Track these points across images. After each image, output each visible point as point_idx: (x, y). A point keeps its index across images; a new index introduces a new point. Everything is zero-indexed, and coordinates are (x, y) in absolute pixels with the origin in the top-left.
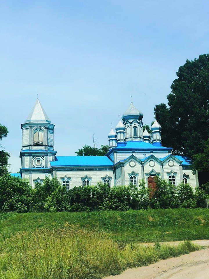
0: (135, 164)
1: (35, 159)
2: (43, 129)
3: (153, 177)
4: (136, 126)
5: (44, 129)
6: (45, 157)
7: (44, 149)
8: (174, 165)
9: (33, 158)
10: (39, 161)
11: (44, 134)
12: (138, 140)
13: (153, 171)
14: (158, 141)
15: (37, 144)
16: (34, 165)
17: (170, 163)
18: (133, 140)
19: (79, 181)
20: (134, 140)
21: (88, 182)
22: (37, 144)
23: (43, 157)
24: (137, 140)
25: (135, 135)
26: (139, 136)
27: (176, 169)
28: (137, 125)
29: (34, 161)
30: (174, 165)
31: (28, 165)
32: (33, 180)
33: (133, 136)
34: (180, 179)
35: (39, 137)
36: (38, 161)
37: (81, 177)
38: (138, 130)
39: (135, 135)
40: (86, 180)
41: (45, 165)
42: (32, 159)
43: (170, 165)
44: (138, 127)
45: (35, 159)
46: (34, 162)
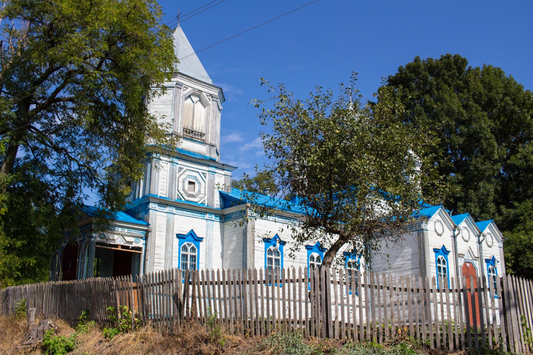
0: (443, 229)
1: (183, 177)
2: (208, 99)
5: (209, 102)
9: (179, 171)
10: (194, 183)
11: (208, 114)
16: (182, 192)
23: (203, 173)
32: (175, 236)
35: (193, 118)
36: (190, 183)
41: (206, 197)
45: (183, 177)
46: (181, 184)
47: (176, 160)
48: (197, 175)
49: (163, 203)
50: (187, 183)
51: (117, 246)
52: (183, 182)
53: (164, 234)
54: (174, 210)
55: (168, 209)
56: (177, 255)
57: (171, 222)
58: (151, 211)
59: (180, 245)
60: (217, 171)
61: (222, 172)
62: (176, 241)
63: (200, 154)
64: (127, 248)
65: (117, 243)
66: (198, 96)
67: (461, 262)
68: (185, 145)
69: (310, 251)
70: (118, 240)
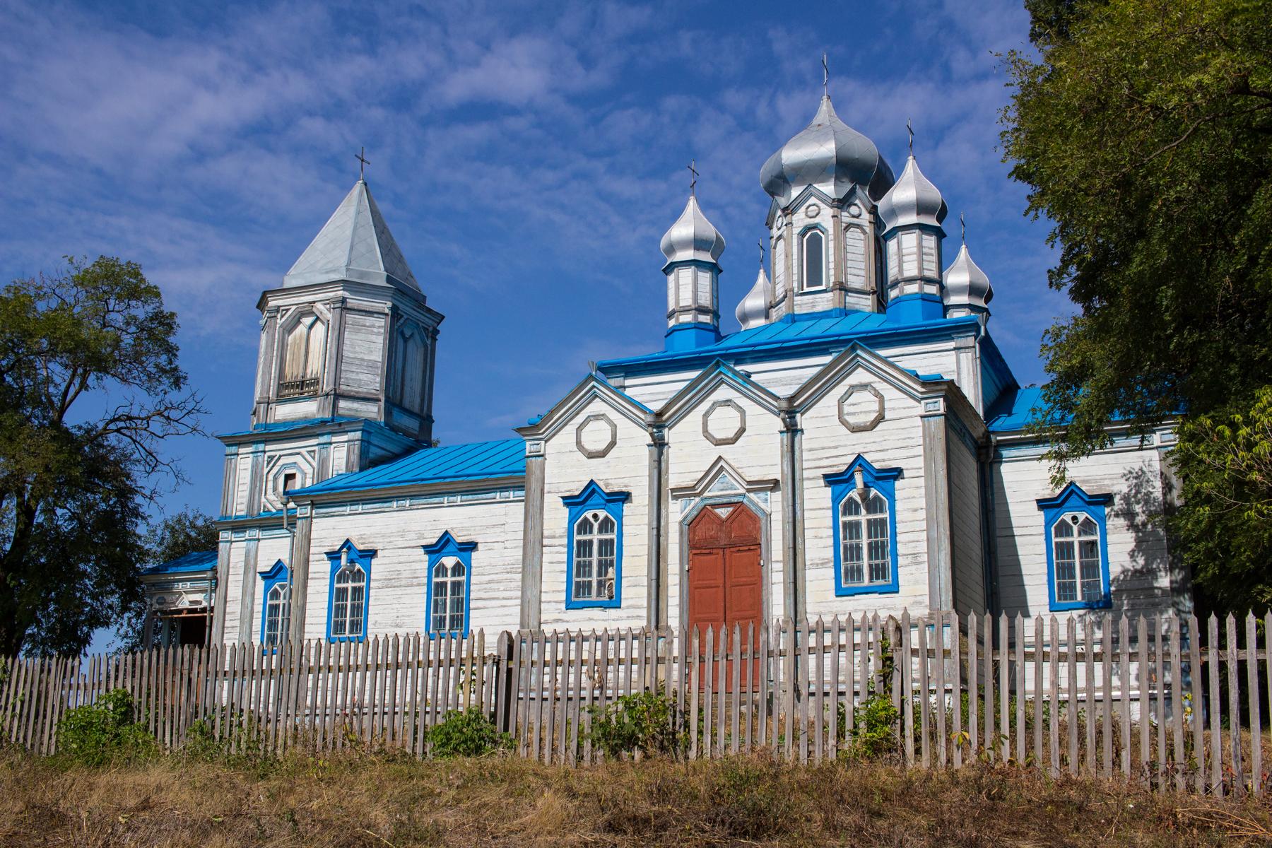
3: (723, 513)
4: (815, 227)
6: (317, 456)
7: (319, 416)
8: (880, 418)
12: (825, 302)
13: (717, 469)
14: (912, 289)
15: (298, 388)
17: (852, 409)
18: (797, 311)
19: (415, 566)
20: (803, 305)
21: (457, 569)
22: (298, 388)
24: (819, 309)
25: (814, 275)
26: (832, 279)
27: (900, 444)
28: (826, 217)
29: (271, 477)
30: (880, 418)
31: (245, 500)
33: (795, 285)
34: (923, 514)
37: (425, 542)
38: (831, 244)
39: (814, 275)
40: (449, 562)
42: (266, 471)
43: (852, 420)
44: (831, 231)
46: (270, 485)
47: (261, 447)
48: (298, 459)
49: (239, 526)
50: (281, 480)
51: (180, 611)
52: (275, 478)
53: (241, 577)
54: (256, 533)
55: (247, 534)
56: (261, 608)
57: (252, 554)
58: (221, 545)
59: (266, 591)
60: (335, 439)
61: (345, 438)
62: (260, 584)
63: (305, 419)
64: (194, 611)
65: (180, 607)
66: (311, 313)
67: (676, 512)
68: (284, 412)
69: (435, 556)
70: (185, 602)
